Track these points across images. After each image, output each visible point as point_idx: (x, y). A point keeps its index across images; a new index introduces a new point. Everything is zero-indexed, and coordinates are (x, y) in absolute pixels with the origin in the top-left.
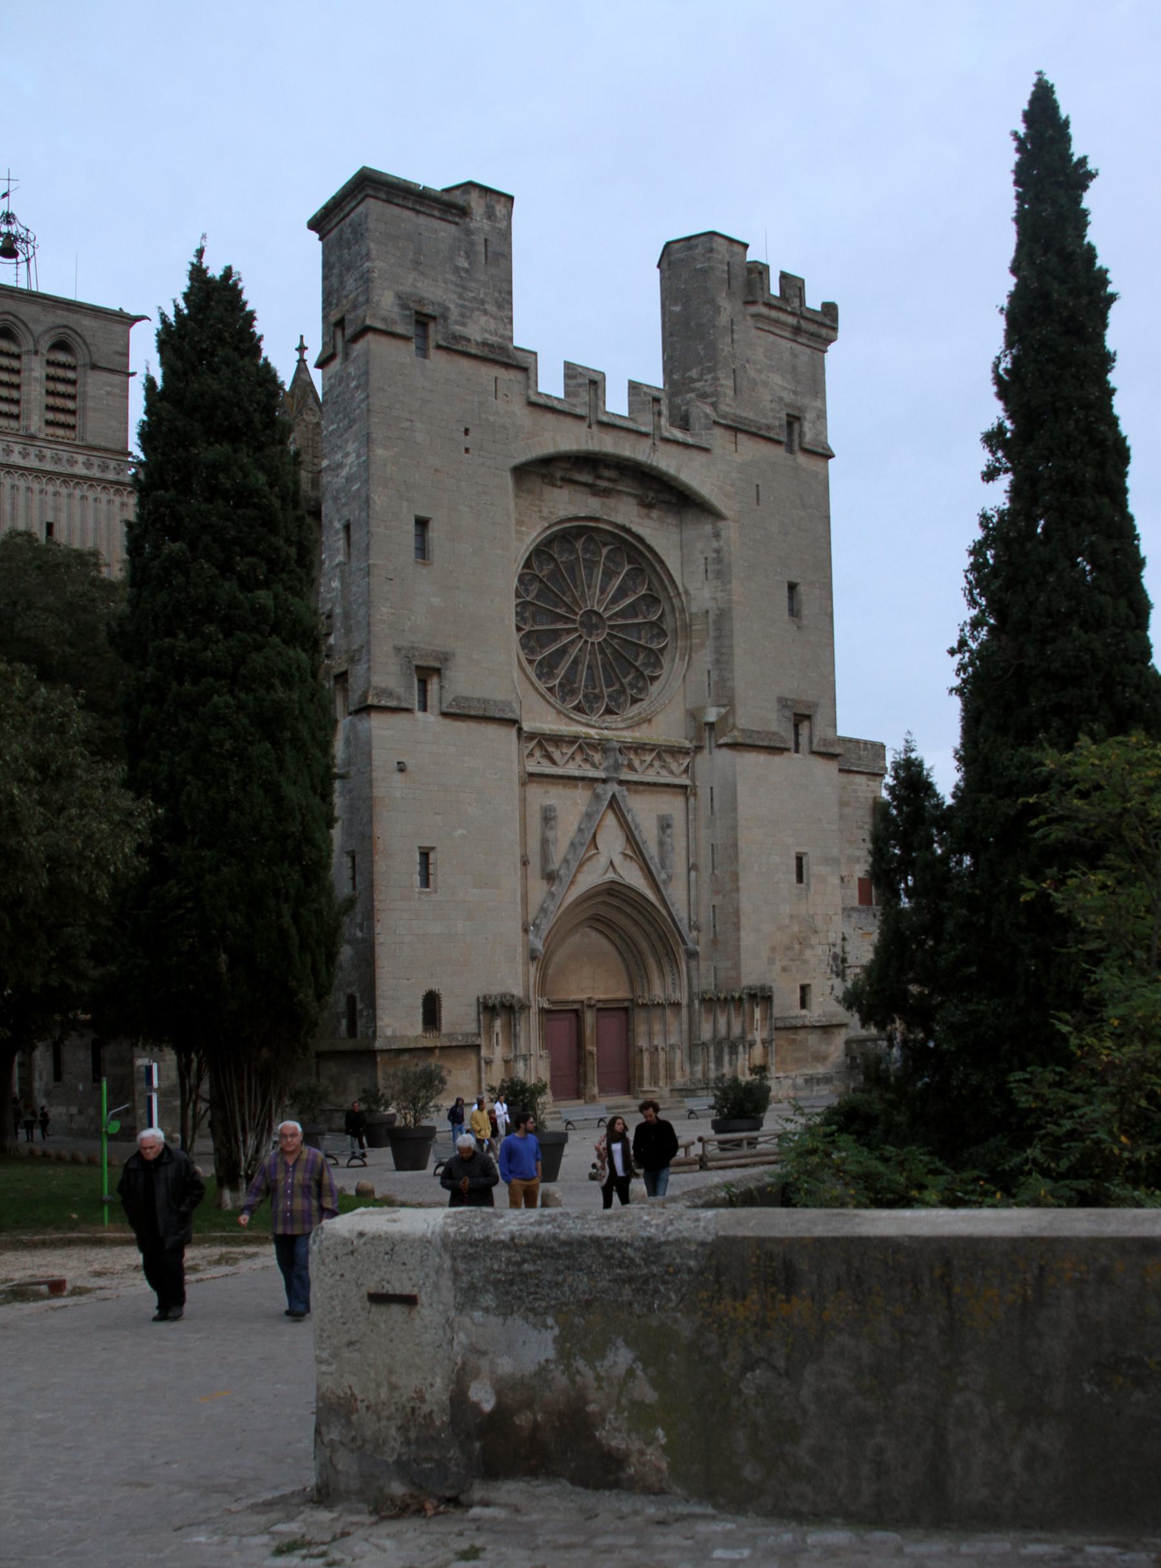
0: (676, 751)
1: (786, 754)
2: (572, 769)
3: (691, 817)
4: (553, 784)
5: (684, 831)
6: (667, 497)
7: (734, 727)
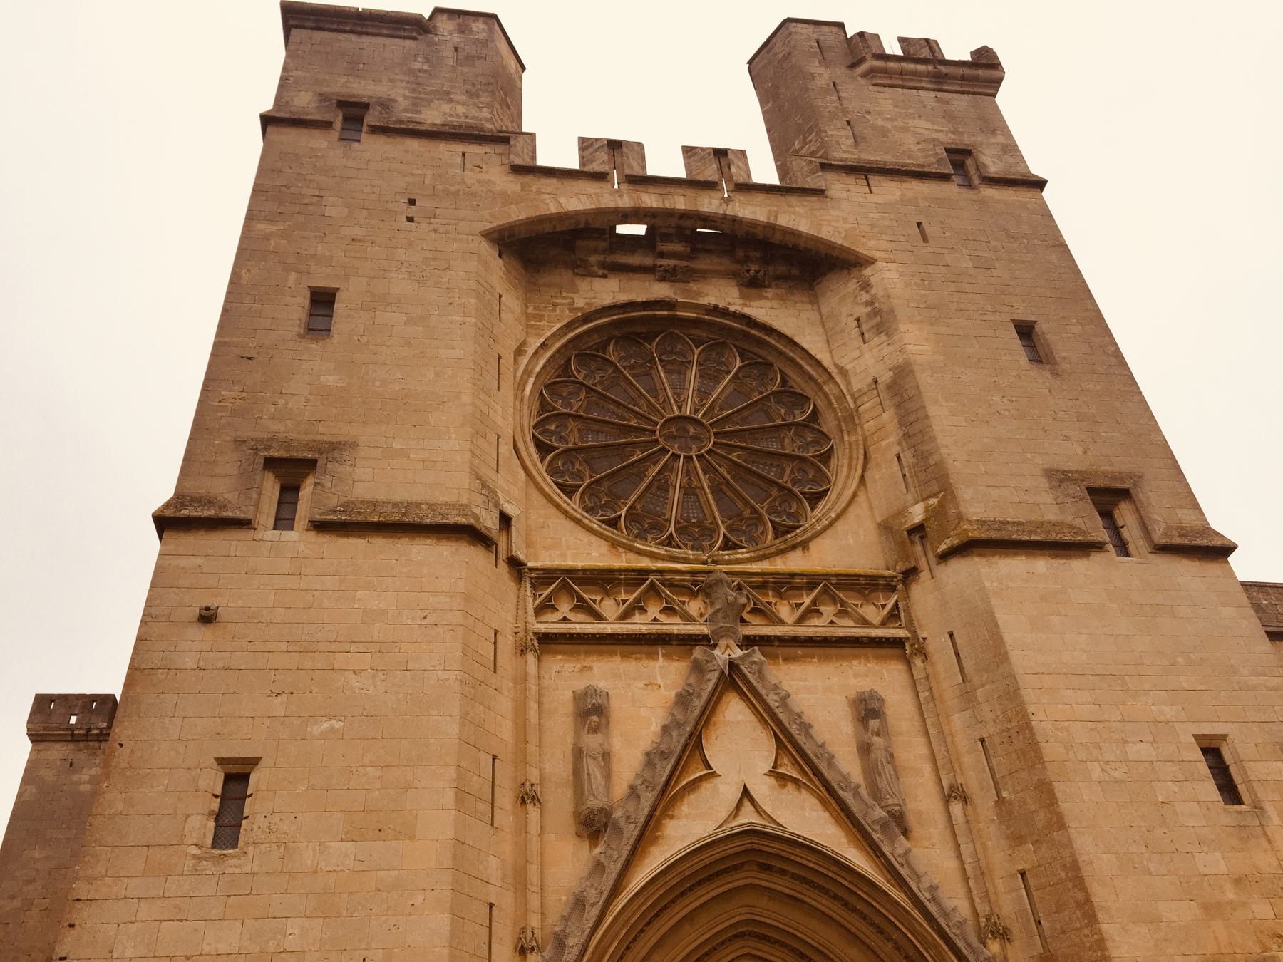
0: (867, 585)
1: (1096, 557)
2: (639, 624)
3: (924, 695)
4: (601, 654)
5: (917, 723)
6: (782, 269)
7: (960, 517)
